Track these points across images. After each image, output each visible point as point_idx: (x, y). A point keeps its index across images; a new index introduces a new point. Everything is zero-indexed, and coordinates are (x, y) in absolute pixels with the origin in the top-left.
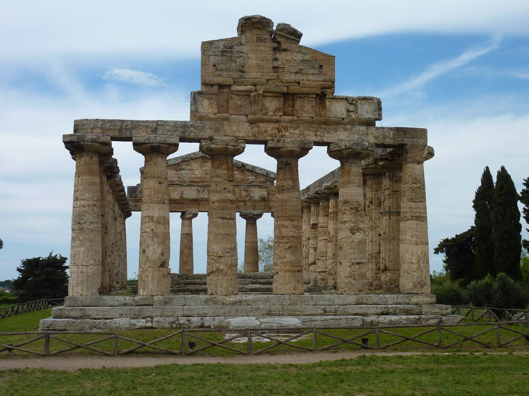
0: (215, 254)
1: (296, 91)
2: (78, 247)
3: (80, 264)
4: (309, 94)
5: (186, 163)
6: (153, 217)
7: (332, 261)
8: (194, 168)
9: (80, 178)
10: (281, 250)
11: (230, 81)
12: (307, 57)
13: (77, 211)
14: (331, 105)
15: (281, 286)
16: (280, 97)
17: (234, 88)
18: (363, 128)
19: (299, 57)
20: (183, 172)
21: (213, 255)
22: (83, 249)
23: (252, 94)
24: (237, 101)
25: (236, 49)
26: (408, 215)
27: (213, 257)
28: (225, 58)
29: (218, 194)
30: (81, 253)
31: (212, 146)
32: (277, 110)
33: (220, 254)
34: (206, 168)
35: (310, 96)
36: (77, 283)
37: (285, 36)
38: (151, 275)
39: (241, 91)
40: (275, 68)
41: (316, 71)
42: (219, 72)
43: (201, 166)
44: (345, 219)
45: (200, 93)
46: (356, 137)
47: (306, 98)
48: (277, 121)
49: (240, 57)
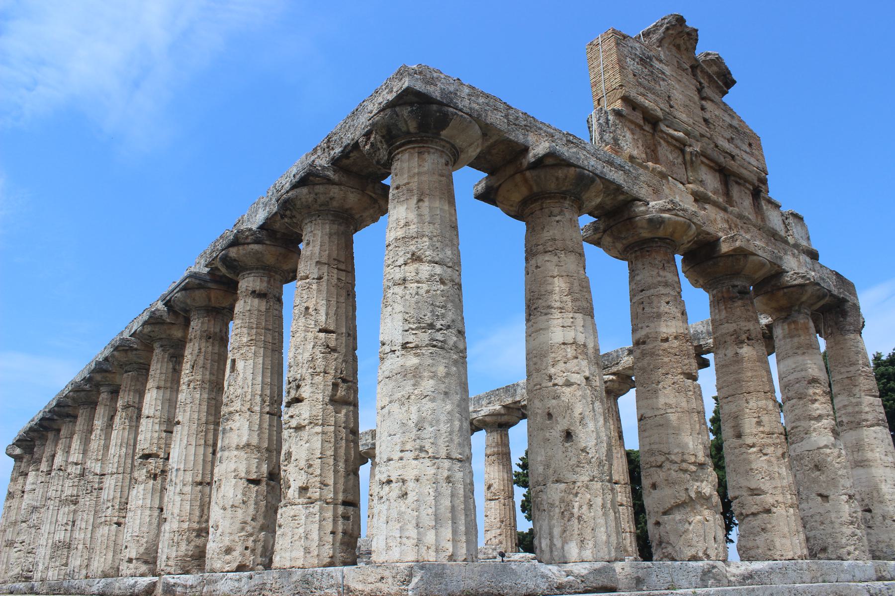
0: (693, 459)
2: (433, 400)
3: (443, 453)
4: (746, 181)
6: (585, 345)
7: (498, 531)
9: (426, 204)
10: (769, 461)
11: (660, 113)
12: (735, 123)
13: (422, 292)
14: (767, 209)
15: (784, 541)
16: (716, 170)
18: (808, 259)
19: (727, 119)
21: (683, 461)
22: (449, 407)
23: (688, 149)
26: (870, 417)
27: (684, 465)
29: (673, 323)
30: (443, 418)
31: (666, 215)
33: (701, 458)
35: (747, 185)
36: (437, 518)
37: (710, 77)
38: (599, 501)
39: (673, 137)
41: (748, 150)
42: (642, 90)
44: (818, 412)
45: (618, 113)
47: (743, 188)
48: (725, 210)
49: (664, 80)
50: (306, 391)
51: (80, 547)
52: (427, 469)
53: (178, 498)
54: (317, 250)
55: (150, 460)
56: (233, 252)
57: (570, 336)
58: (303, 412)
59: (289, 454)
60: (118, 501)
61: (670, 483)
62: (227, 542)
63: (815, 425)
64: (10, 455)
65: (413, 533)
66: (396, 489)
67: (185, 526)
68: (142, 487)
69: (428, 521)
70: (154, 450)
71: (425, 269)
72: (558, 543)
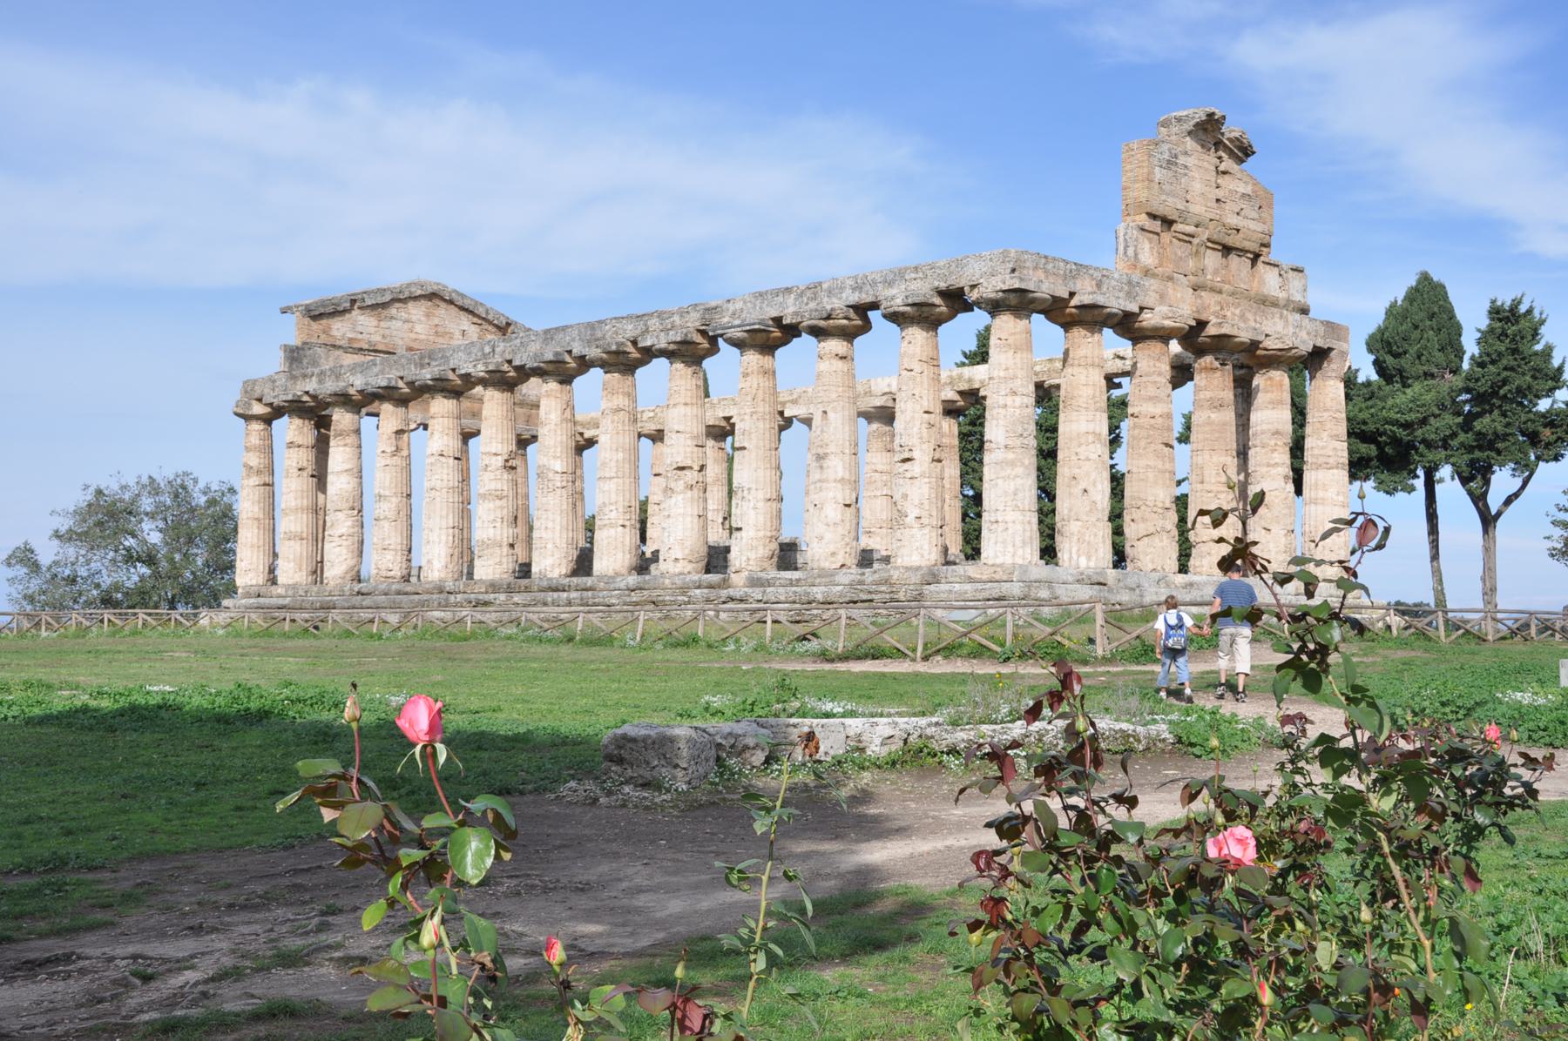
1: (1238, 245)
5: (397, 305)
8: (414, 318)
17: (1178, 227)
18: (1297, 316)
20: (396, 324)
24: (1180, 249)
25: (1182, 160)
26: (1331, 460)
28: (1171, 173)
32: (1216, 272)
34: (436, 321)
40: (1218, 200)
43: (428, 315)
46: (1291, 330)
48: (1220, 292)
50: (916, 454)
51: (550, 546)
52: (1018, 516)
53: (752, 512)
54: (918, 350)
55: (686, 472)
56: (822, 323)
57: (1091, 427)
58: (915, 468)
59: (905, 496)
60: (621, 504)
61: (1144, 520)
62: (832, 548)
63: (1274, 471)
64: (248, 418)
65: (1010, 549)
66: (1001, 527)
67: (761, 534)
68: (680, 497)
69: (1018, 543)
70: (689, 463)
71: (1018, 400)
72: (1075, 556)
